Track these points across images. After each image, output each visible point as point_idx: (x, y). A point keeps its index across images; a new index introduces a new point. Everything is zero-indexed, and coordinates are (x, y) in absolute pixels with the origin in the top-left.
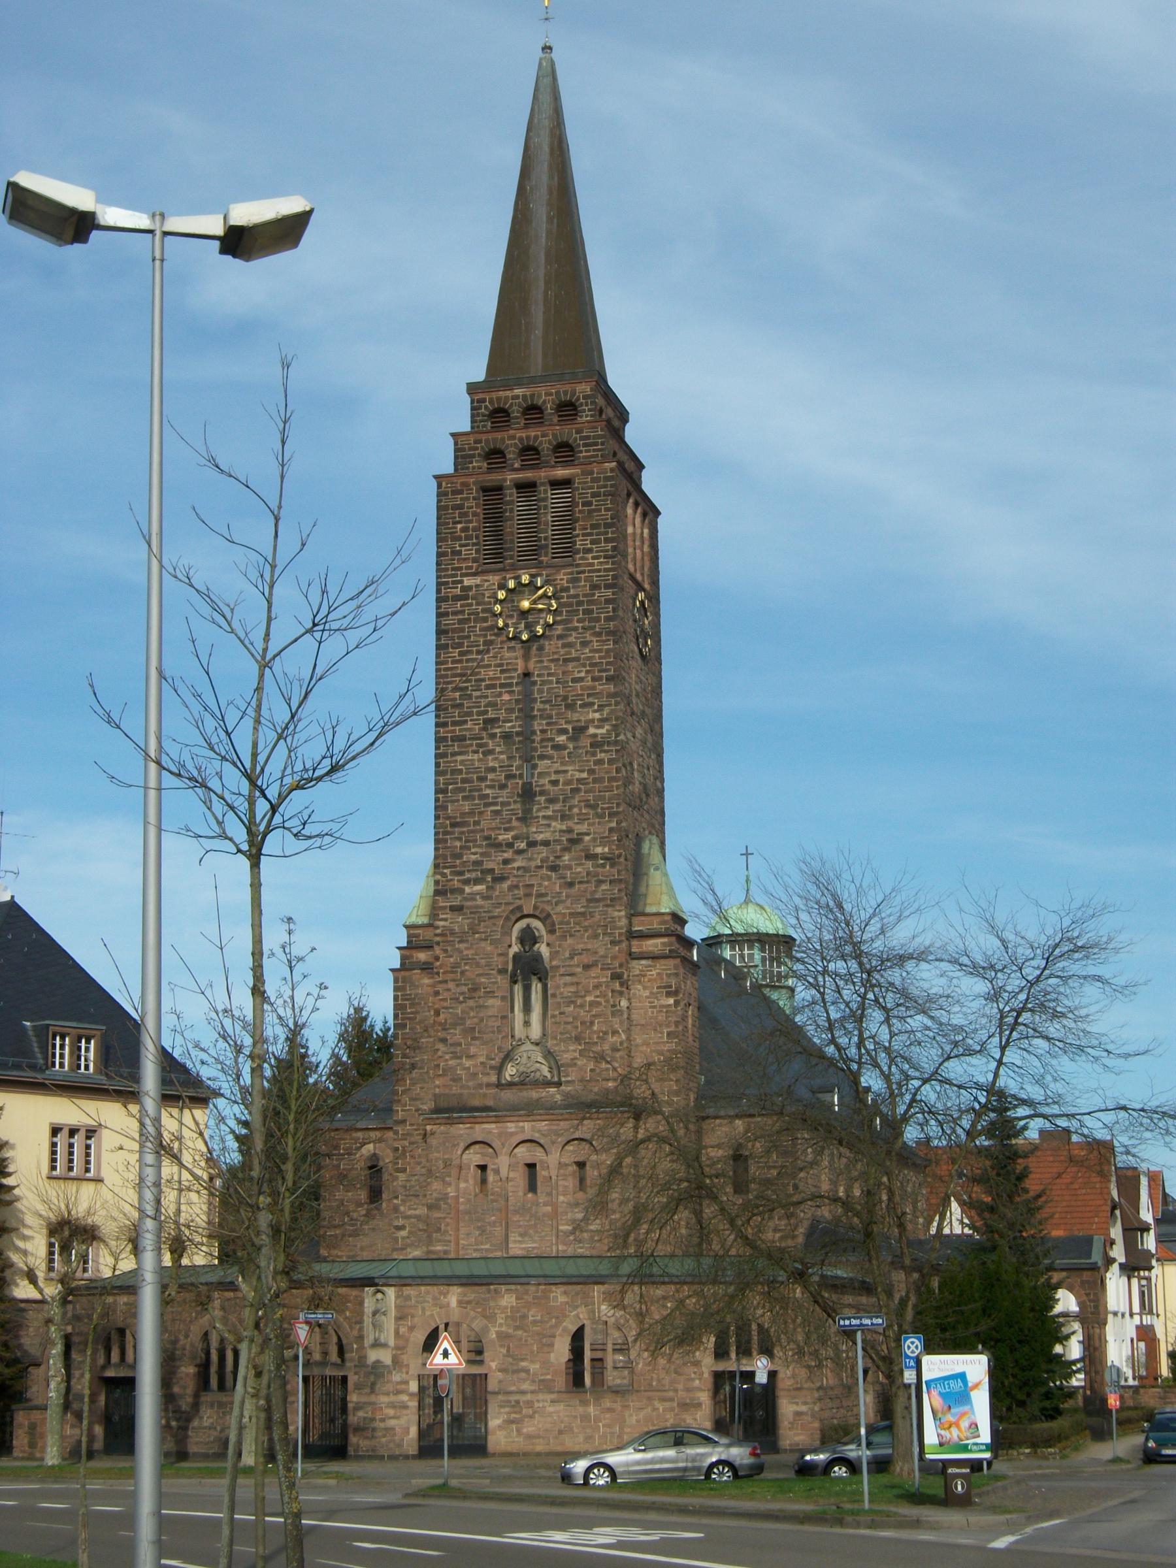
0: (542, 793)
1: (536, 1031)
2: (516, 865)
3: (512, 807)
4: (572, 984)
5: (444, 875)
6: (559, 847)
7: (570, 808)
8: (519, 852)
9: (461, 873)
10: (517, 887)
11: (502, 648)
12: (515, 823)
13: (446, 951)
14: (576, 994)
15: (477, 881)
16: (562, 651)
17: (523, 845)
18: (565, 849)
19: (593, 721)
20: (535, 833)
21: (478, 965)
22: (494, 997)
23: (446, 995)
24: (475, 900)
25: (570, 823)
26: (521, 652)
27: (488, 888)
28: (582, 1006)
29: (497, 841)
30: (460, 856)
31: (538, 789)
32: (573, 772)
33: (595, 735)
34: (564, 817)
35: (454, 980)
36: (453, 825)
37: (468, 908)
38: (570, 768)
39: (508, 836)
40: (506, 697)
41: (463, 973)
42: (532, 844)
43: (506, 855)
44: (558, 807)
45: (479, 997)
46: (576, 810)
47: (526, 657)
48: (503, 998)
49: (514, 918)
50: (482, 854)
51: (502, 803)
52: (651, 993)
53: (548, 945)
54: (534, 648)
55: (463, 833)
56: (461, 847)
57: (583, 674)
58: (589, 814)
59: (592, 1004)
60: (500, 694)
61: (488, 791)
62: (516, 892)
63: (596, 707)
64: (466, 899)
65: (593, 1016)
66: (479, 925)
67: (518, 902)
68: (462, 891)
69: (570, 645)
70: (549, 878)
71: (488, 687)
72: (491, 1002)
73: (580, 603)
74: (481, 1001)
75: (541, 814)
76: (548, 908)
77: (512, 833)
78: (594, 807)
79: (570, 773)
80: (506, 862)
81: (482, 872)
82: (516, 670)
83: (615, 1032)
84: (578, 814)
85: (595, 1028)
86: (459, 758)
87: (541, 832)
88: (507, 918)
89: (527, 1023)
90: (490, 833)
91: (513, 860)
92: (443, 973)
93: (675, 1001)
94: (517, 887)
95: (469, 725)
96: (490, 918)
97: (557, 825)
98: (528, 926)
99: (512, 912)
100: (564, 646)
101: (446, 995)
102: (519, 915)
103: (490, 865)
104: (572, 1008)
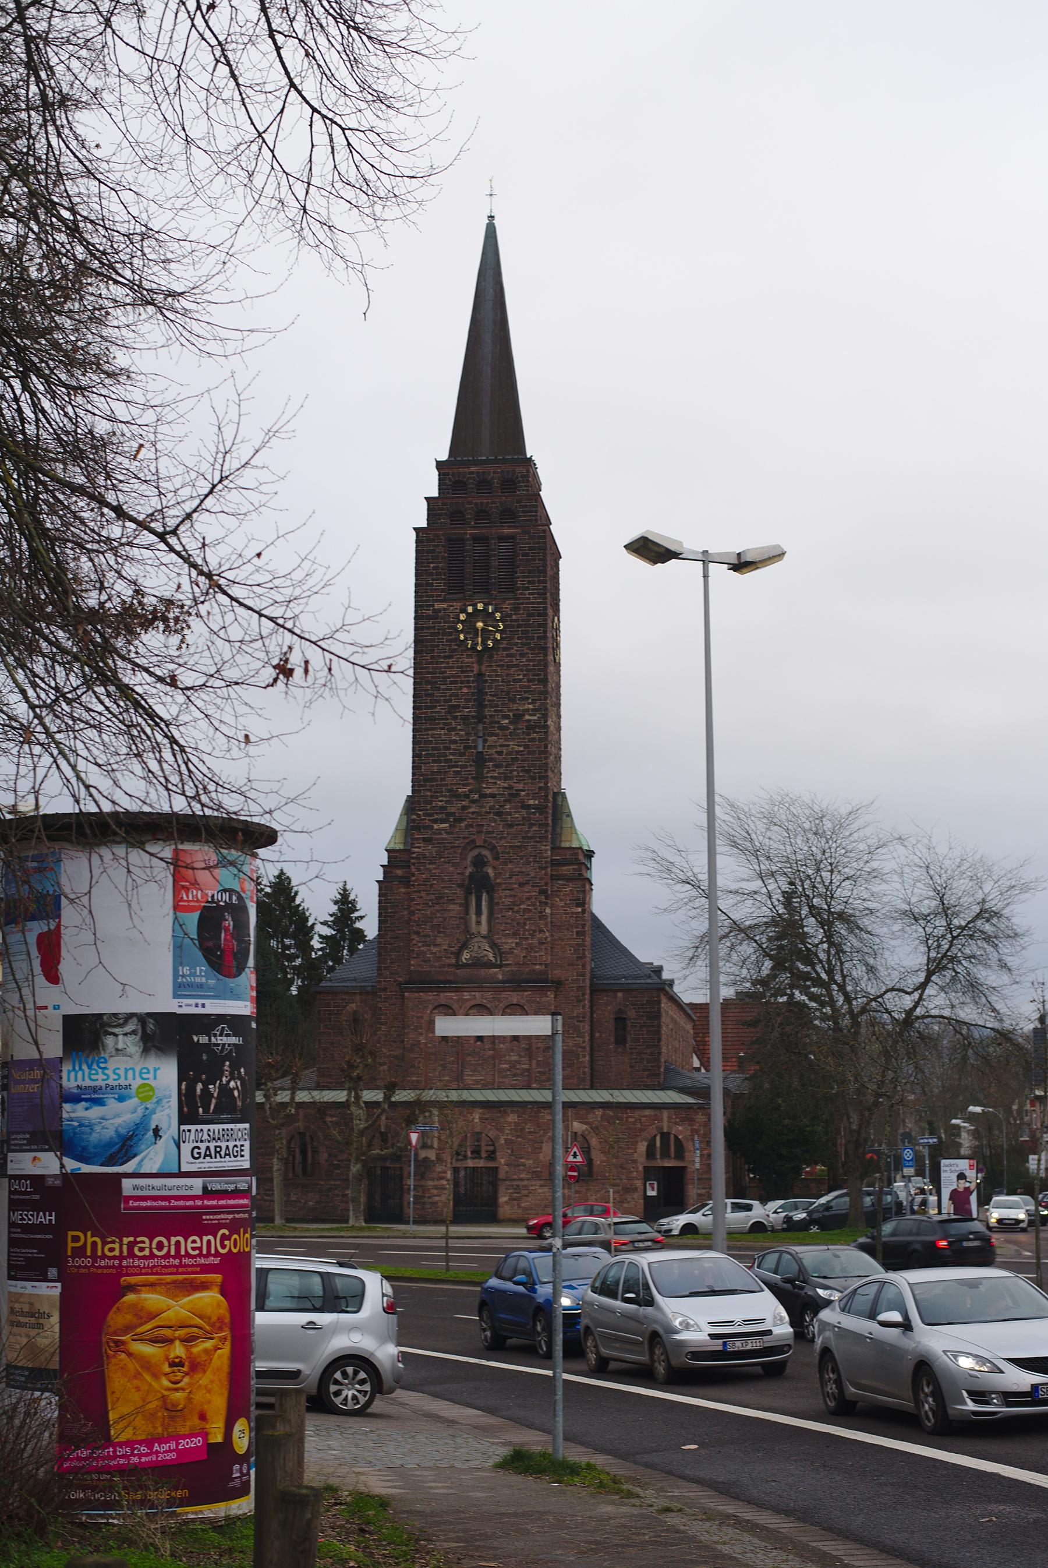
1: (484, 929)
7: (511, 772)
8: (474, 801)
9: (431, 815)
12: (471, 781)
13: (419, 870)
14: (514, 903)
15: (443, 821)
18: (508, 801)
19: (528, 710)
21: (443, 880)
25: (511, 782)
28: (518, 912)
32: (514, 746)
33: (529, 721)
34: (506, 778)
36: (426, 780)
39: (466, 790)
40: (465, 690)
42: (483, 796)
46: (515, 773)
47: (480, 663)
48: (460, 905)
50: (446, 802)
59: (525, 910)
60: (461, 688)
61: (451, 757)
64: (434, 833)
69: (512, 655)
70: (495, 821)
72: (452, 907)
76: (494, 842)
78: (528, 771)
80: (464, 808)
81: (447, 814)
83: (541, 931)
86: (430, 732)
88: (464, 848)
89: (479, 923)
91: (469, 807)
94: (471, 826)
97: (501, 783)
98: (480, 855)
100: (508, 656)
103: (453, 810)
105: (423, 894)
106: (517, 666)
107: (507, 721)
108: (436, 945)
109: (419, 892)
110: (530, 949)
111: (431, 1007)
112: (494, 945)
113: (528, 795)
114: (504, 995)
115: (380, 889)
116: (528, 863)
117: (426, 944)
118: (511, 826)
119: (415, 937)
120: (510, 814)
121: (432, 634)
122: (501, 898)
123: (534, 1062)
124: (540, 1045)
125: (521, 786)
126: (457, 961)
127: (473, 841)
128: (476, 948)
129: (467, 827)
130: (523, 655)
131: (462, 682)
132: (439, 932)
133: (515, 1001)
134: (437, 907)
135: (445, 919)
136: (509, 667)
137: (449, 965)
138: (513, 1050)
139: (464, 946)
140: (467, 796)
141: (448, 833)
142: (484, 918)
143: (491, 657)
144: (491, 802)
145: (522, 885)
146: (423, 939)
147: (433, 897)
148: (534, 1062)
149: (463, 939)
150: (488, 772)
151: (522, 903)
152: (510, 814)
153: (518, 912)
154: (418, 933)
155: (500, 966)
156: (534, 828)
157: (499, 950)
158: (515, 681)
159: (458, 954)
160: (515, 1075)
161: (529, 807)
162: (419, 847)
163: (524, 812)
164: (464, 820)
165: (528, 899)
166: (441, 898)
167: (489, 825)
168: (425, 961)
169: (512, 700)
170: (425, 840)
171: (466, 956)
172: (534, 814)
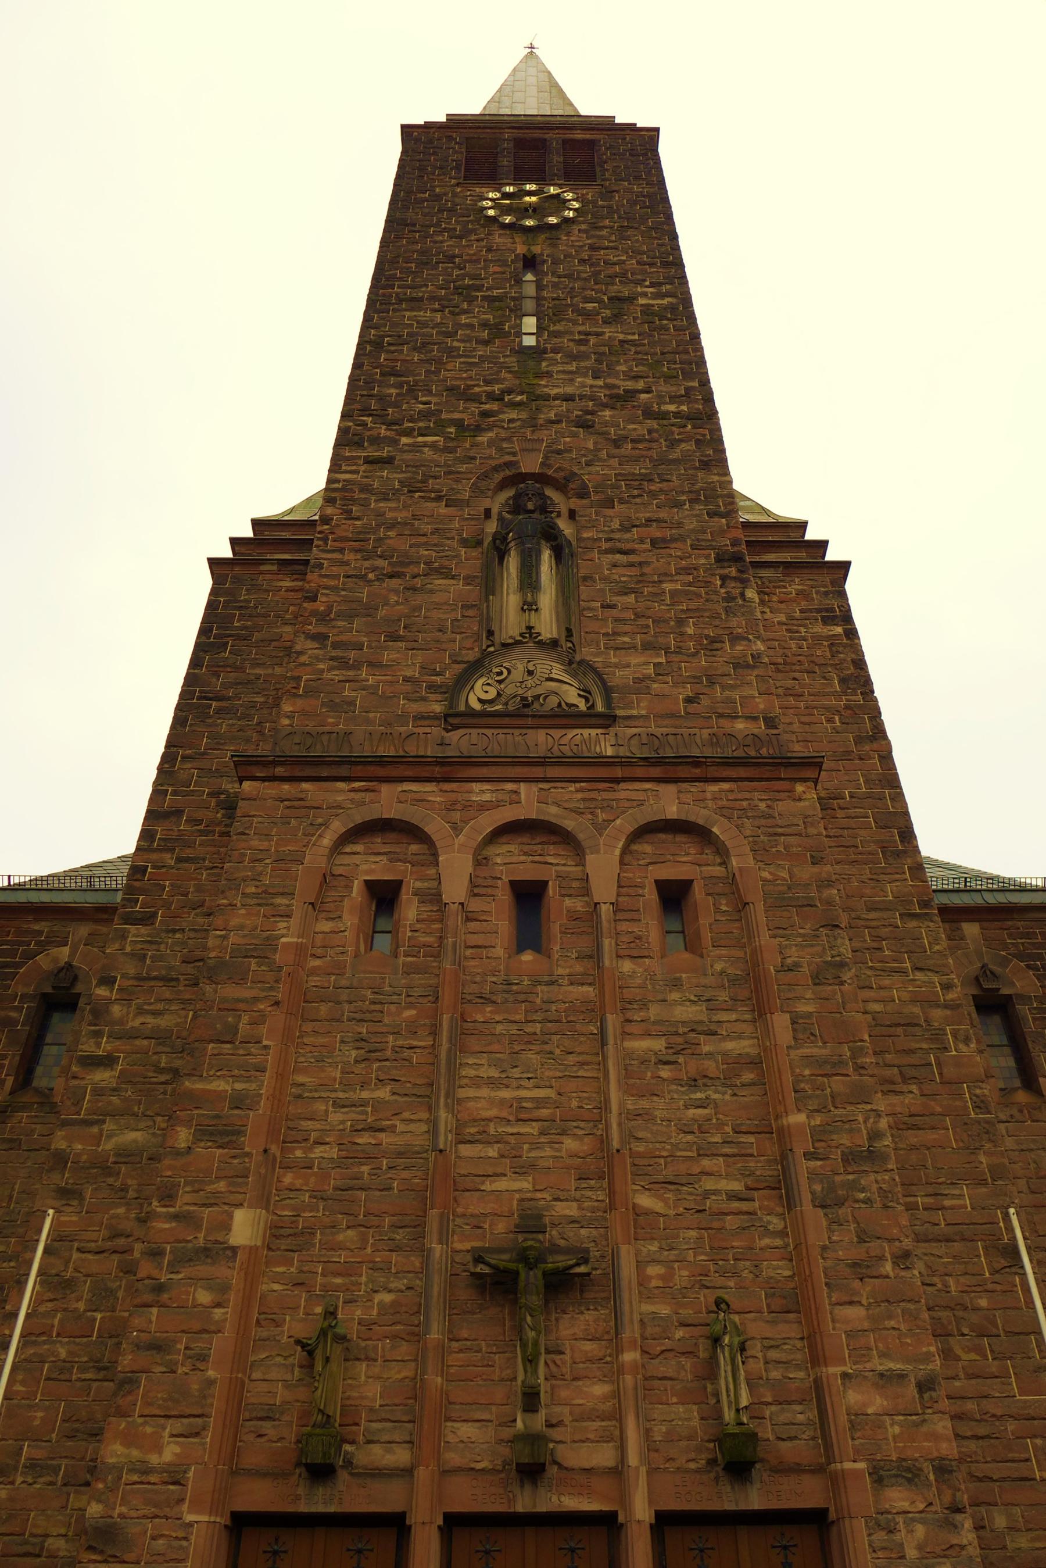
0: (555, 351)
1: (547, 625)
4: (632, 565)
11: (491, 235)
14: (642, 578)
18: (605, 406)
20: (546, 386)
30: (397, 405)
38: (607, 330)
39: (497, 388)
48: (468, 580)
49: (498, 477)
52: (791, 618)
53: (572, 515)
55: (408, 383)
56: (398, 395)
63: (647, 283)
68: (395, 442)
74: (418, 582)
76: (575, 469)
80: (485, 414)
86: (407, 314)
88: (485, 476)
90: (458, 383)
91: (501, 411)
108: (374, 665)
109: (341, 550)
111: (338, 827)
114: (626, 791)
123: (780, 1022)
124: (793, 955)
125: (641, 385)
128: (518, 673)
129: (491, 443)
133: (672, 811)
134: (394, 583)
137: (419, 717)
138: (676, 984)
139: (474, 669)
142: (547, 599)
148: (780, 1022)
155: (607, 720)
157: (604, 683)
160: (693, 1083)
161: (663, 416)
163: (653, 424)
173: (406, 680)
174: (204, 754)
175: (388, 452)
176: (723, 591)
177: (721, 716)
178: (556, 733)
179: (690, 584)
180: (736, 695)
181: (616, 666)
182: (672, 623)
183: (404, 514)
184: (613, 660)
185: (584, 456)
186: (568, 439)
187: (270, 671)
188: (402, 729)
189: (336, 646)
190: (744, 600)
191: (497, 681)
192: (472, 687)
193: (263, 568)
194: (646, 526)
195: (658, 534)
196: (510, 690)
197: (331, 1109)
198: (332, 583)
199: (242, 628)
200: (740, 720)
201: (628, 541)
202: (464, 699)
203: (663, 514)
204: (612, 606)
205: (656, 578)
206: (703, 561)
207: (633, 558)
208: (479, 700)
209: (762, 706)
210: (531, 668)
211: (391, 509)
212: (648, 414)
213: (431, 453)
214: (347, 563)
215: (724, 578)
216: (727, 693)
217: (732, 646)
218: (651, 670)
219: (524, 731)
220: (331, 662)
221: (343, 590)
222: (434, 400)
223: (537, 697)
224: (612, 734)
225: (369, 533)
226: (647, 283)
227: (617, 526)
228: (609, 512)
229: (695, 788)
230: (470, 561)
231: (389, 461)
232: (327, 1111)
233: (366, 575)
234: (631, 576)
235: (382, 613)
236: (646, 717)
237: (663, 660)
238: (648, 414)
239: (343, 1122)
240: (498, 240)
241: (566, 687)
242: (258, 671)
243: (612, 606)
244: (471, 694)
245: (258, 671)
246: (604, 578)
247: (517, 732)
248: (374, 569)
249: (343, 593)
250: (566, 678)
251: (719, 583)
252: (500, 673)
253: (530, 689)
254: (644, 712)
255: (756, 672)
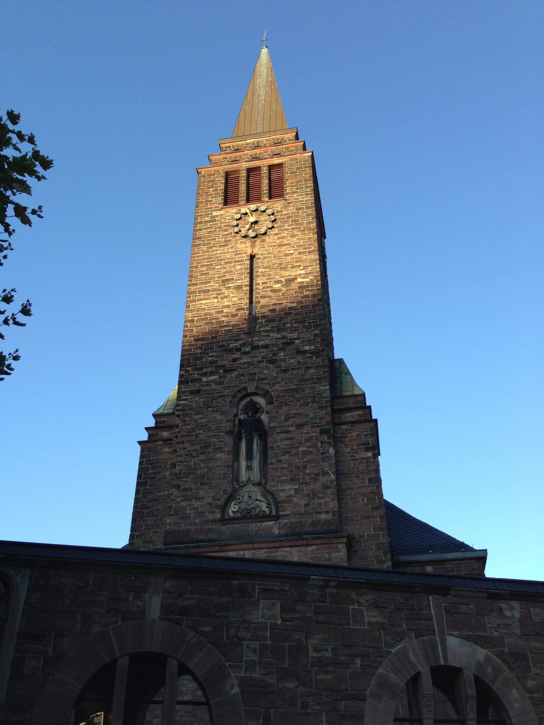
1: (256, 475)
2: (242, 361)
3: (241, 327)
5: (187, 371)
6: (276, 348)
7: (284, 324)
8: (246, 353)
10: (243, 375)
11: (237, 243)
12: (242, 336)
15: (211, 374)
16: (278, 241)
17: (248, 349)
19: (300, 275)
22: (223, 452)
23: (181, 452)
24: (211, 386)
25: (284, 334)
26: (250, 244)
27: (220, 377)
28: (295, 455)
29: (229, 348)
30: (201, 359)
31: (260, 315)
34: (279, 330)
35: (189, 441)
37: (204, 391)
39: (238, 344)
40: (239, 267)
41: (197, 435)
42: (257, 347)
43: (235, 356)
44: (275, 324)
45: (209, 453)
46: (289, 325)
47: (253, 246)
48: (229, 452)
49: (240, 396)
50: (216, 357)
51: (233, 325)
52: (352, 449)
54: (258, 241)
56: (201, 353)
57: (292, 252)
58: (299, 327)
59: (304, 453)
60: (235, 266)
62: (242, 378)
63: (302, 268)
64: (203, 386)
65: (306, 462)
66: (212, 402)
67: (245, 385)
69: (283, 238)
70: (268, 368)
71: (226, 263)
72: (219, 455)
73: (288, 218)
74: (211, 455)
75: (262, 329)
76: (268, 388)
77: (240, 342)
79: (284, 304)
80: (235, 360)
81: (217, 367)
82: (247, 253)
83: (325, 474)
84: (290, 328)
85: (308, 471)
86: (203, 302)
87: (263, 340)
88: (235, 396)
91: (241, 358)
92: (181, 437)
93: (373, 454)
94: (243, 375)
95: (212, 284)
96: (221, 396)
99: (239, 391)
100: (279, 238)
101: (181, 452)
102: (244, 393)
103: (223, 363)
104: (287, 457)
105: (186, 445)
106: (289, 244)
107: (279, 285)
108: (198, 499)
109: (183, 442)
110: (313, 495)
112: (267, 493)
113: (303, 342)
115: (142, 451)
116: (306, 404)
117: (187, 498)
118: (286, 371)
119: (174, 491)
120: (285, 360)
121: (209, 232)
122: (276, 441)
125: (295, 335)
126: (223, 516)
127: (245, 389)
128: (246, 499)
129: (237, 377)
130: (293, 236)
131: (235, 262)
132: (203, 484)
134: (202, 457)
135: (211, 469)
136: (280, 246)
137: (213, 521)
139: (231, 497)
140: (238, 349)
141: (217, 383)
142: (256, 463)
143: (264, 241)
144: (264, 352)
145: (299, 426)
146: (184, 493)
147: (197, 447)
149: (230, 489)
150: (260, 327)
151: (300, 444)
152: (285, 360)
153: (295, 455)
154: (178, 487)
155: (277, 518)
156: (312, 371)
157: (275, 499)
158: (285, 255)
159: (225, 507)
161: (305, 352)
162: (186, 400)
163: (300, 358)
164: (236, 370)
165: (308, 440)
166: (206, 447)
167: (261, 373)
168: (183, 518)
169: (285, 269)
170: (192, 392)
171: (233, 508)
172: (311, 357)
173: (208, 503)
174: (144, 534)
175: (198, 387)
176: (321, 449)
177: (316, 513)
178: (259, 524)
179: (309, 447)
180: (322, 501)
181: (280, 490)
182: (301, 468)
183: (205, 420)
184: (280, 488)
185: (272, 380)
186: (266, 372)
187: (163, 493)
188: (207, 527)
189: (184, 490)
190: (329, 454)
191: (239, 502)
192: (230, 506)
193: (158, 443)
194: (294, 417)
195: (299, 422)
196: (243, 506)
197: (189, 682)
198: (181, 459)
199: (152, 474)
200: (323, 514)
201: (288, 426)
202: (227, 511)
203: (301, 411)
204: (280, 461)
205: (297, 445)
206: (314, 434)
207: (289, 435)
208: (233, 512)
209: (331, 506)
210: (250, 495)
211: (201, 418)
212: (299, 352)
213: (214, 385)
214: (185, 448)
215: (322, 442)
216: (320, 501)
217: (323, 477)
218: (292, 492)
219: (248, 524)
220: (182, 498)
221: (185, 462)
222: (215, 354)
223: (252, 509)
224: (278, 524)
225: (192, 432)
226: (302, 268)
227: (283, 419)
228: (281, 411)
229: (304, 549)
230: (229, 440)
231: (198, 392)
232: (188, 683)
233: (192, 454)
234: (287, 445)
235: (199, 472)
236: (289, 515)
237: (297, 487)
238: (299, 352)
239: (193, 687)
240: (240, 246)
241: (262, 503)
242: (159, 494)
243: (280, 461)
244: (230, 509)
245: (159, 494)
246: (278, 446)
247: (245, 525)
248: (195, 450)
249: (185, 463)
250: (262, 499)
251: (320, 445)
252: (239, 499)
253: (250, 505)
254: (289, 513)
255: (330, 490)
